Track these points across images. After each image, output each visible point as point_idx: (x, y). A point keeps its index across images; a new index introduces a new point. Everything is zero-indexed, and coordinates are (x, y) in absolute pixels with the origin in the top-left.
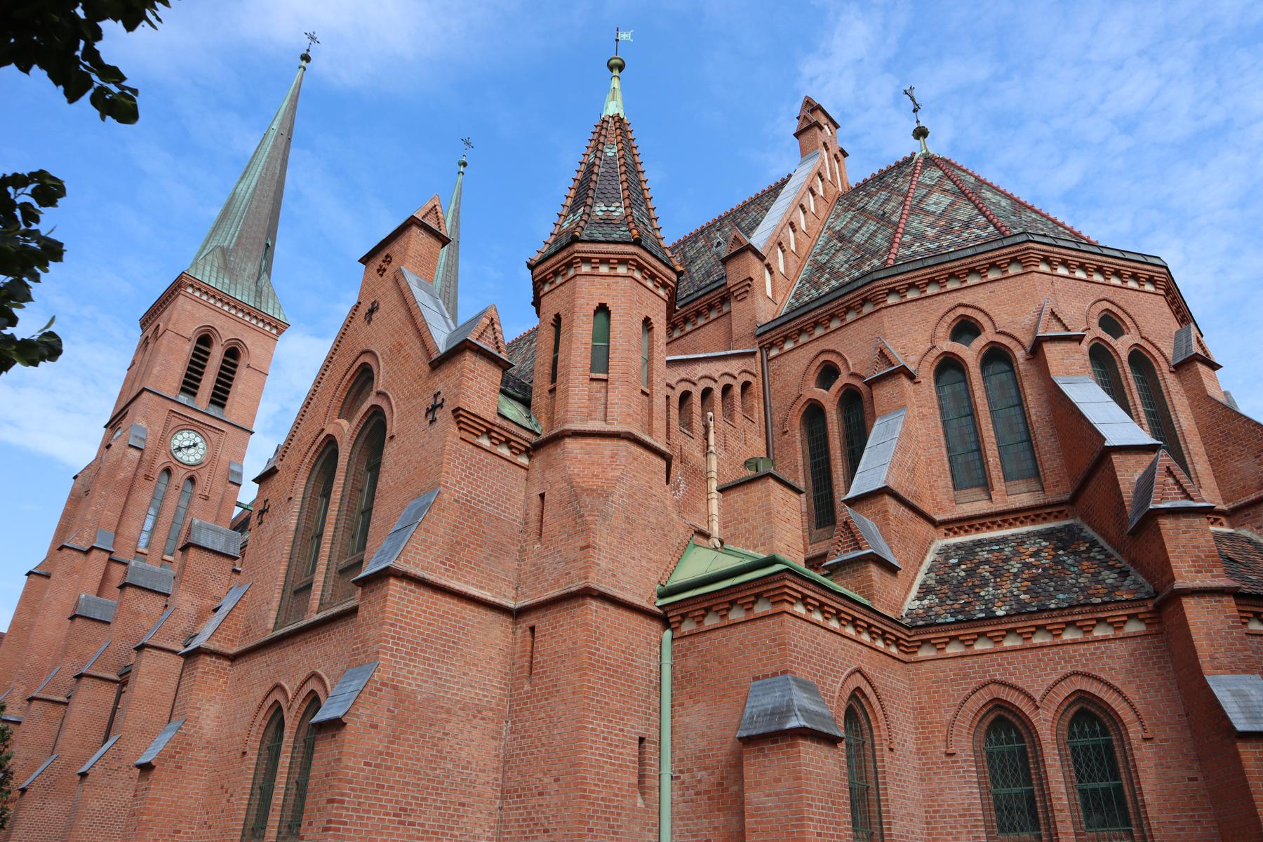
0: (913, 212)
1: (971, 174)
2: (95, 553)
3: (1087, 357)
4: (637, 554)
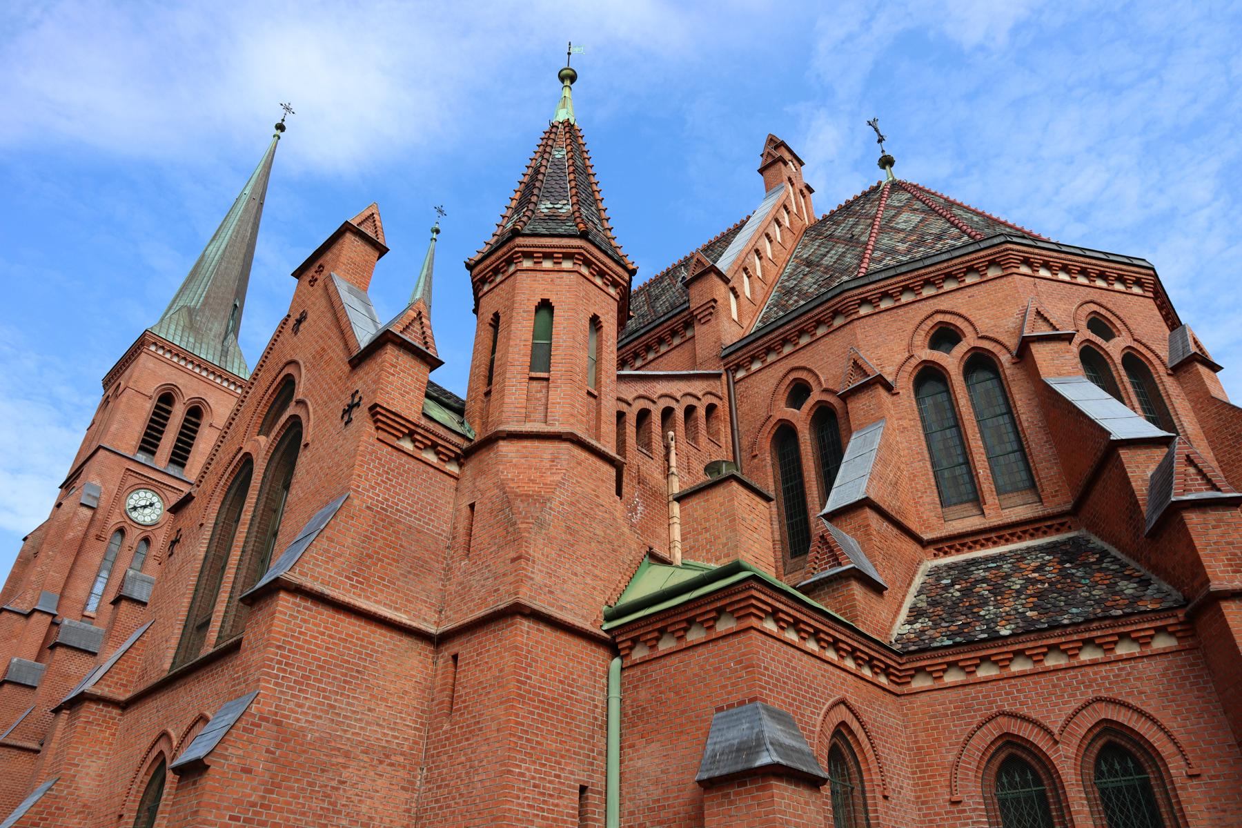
0: (882, 230)
1: (941, 197)
2: (36, 616)
3: (1078, 360)
4: (579, 570)
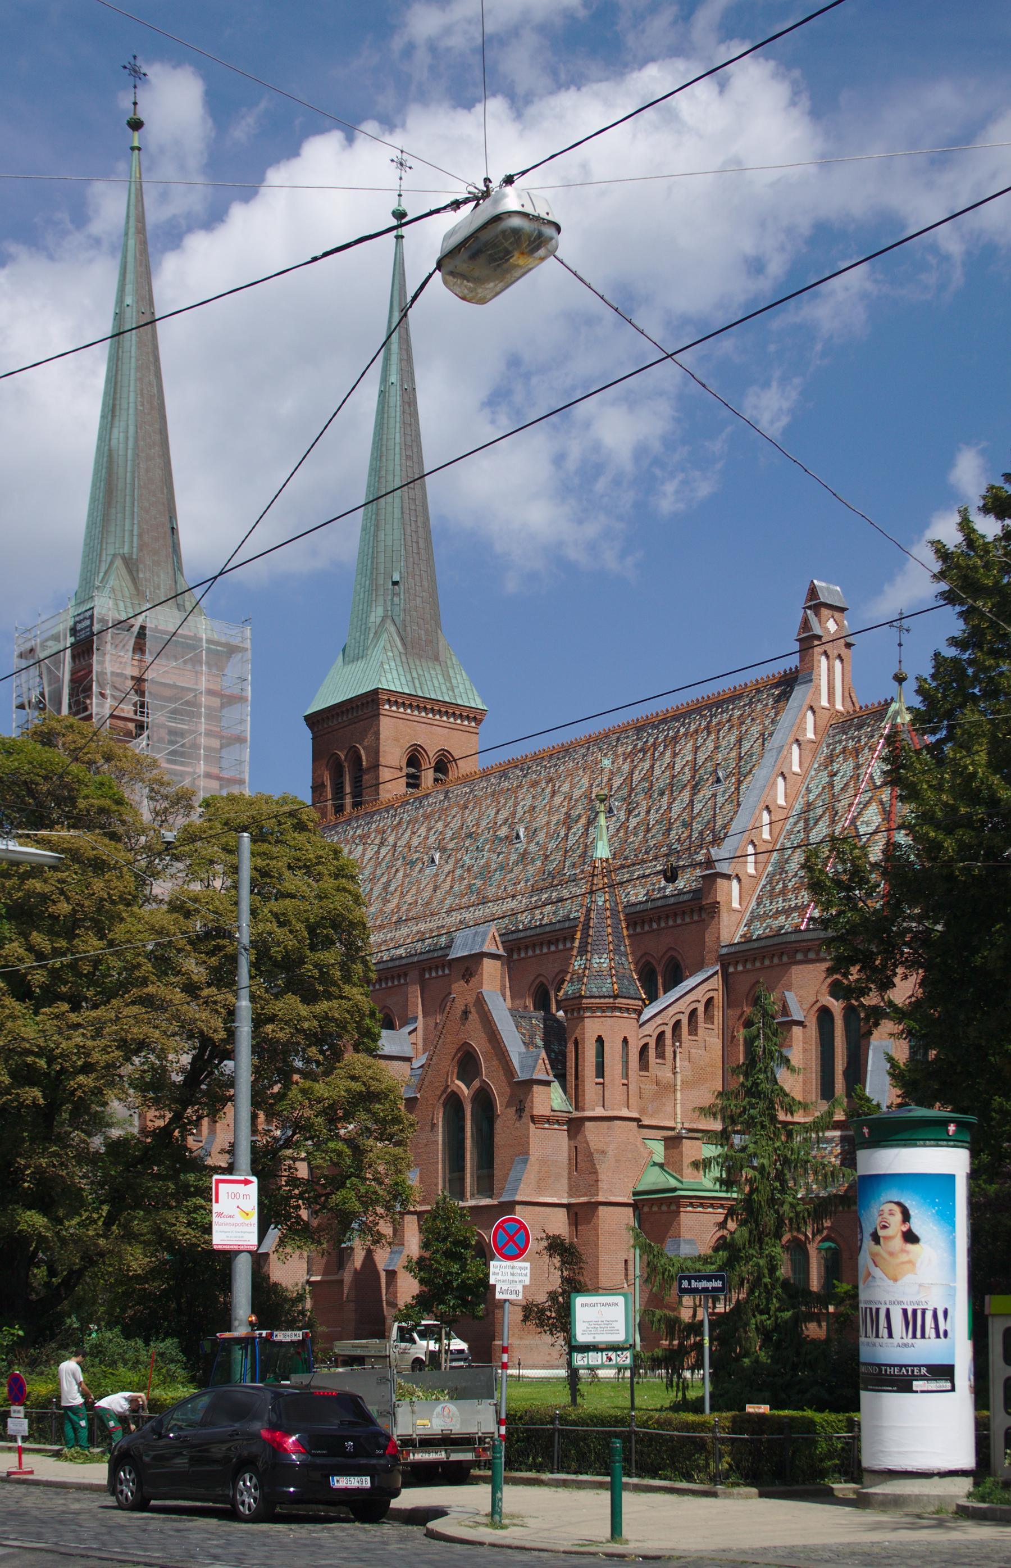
4: (621, 1176)
